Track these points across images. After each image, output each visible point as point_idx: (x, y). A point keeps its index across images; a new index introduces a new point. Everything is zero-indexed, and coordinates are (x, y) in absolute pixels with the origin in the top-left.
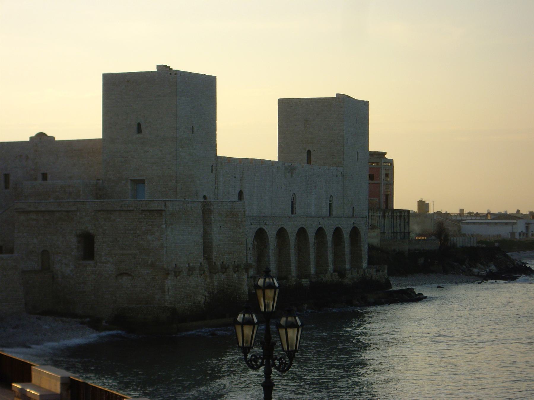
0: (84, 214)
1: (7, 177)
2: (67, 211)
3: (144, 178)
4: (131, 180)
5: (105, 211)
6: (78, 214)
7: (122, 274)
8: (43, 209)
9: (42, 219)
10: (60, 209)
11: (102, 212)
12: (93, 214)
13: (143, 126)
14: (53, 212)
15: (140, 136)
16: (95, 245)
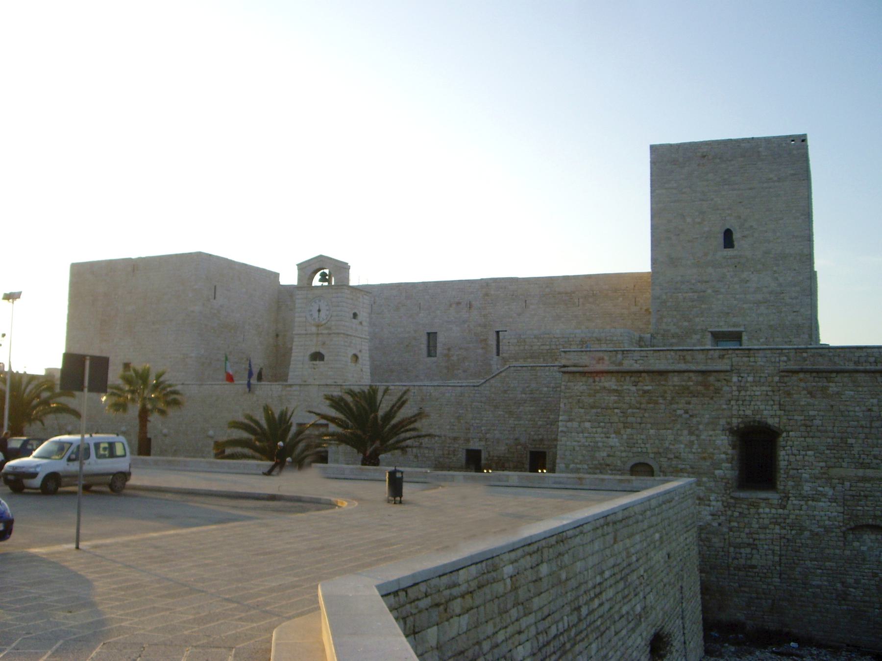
0: (750, 379)
1: (432, 337)
2: (703, 372)
3: (742, 329)
4: (712, 333)
5: (811, 372)
6: (735, 379)
7: (859, 528)
8: (636, 367)
9: (634, 388)
10: (682, 366)
11: (801, 375)
12: (777, 379)
13: (736, 236)
14: (661, 373)
15: (729, 252)
16: (782, 453)
